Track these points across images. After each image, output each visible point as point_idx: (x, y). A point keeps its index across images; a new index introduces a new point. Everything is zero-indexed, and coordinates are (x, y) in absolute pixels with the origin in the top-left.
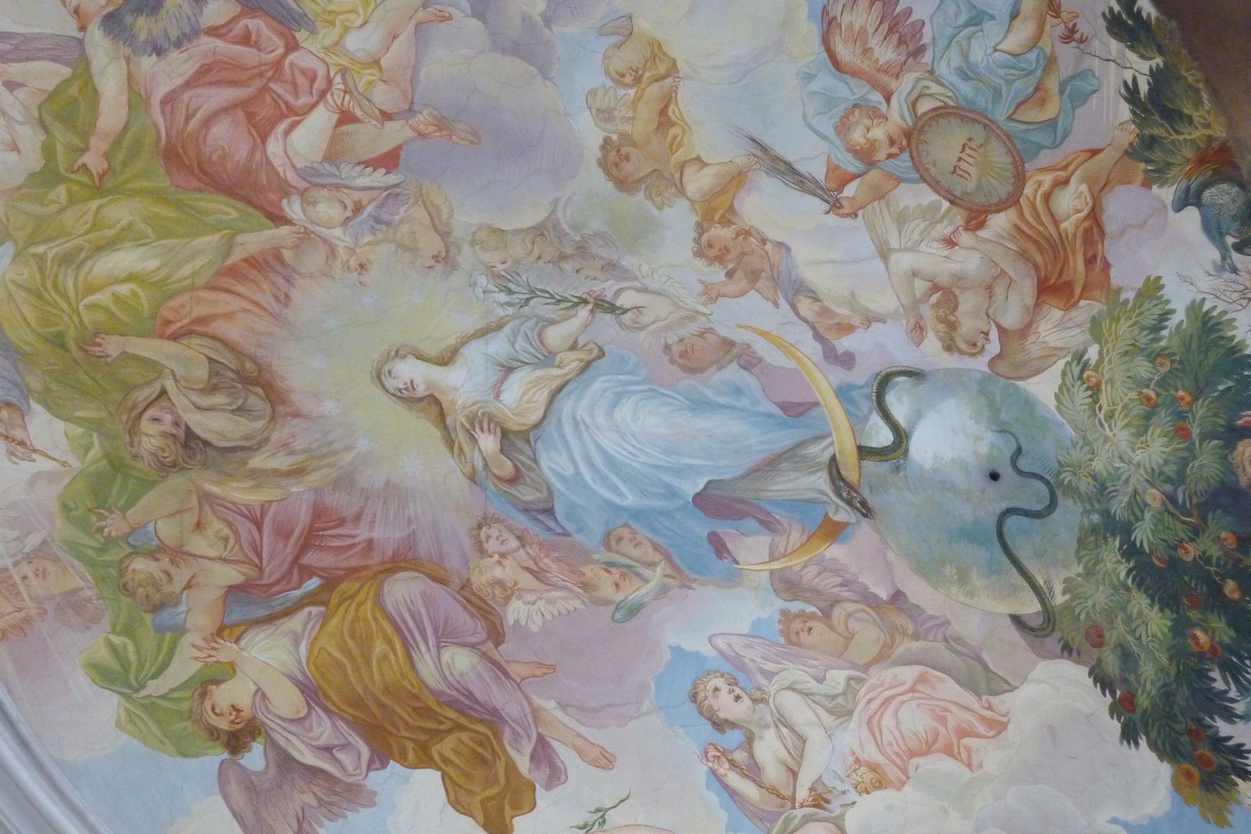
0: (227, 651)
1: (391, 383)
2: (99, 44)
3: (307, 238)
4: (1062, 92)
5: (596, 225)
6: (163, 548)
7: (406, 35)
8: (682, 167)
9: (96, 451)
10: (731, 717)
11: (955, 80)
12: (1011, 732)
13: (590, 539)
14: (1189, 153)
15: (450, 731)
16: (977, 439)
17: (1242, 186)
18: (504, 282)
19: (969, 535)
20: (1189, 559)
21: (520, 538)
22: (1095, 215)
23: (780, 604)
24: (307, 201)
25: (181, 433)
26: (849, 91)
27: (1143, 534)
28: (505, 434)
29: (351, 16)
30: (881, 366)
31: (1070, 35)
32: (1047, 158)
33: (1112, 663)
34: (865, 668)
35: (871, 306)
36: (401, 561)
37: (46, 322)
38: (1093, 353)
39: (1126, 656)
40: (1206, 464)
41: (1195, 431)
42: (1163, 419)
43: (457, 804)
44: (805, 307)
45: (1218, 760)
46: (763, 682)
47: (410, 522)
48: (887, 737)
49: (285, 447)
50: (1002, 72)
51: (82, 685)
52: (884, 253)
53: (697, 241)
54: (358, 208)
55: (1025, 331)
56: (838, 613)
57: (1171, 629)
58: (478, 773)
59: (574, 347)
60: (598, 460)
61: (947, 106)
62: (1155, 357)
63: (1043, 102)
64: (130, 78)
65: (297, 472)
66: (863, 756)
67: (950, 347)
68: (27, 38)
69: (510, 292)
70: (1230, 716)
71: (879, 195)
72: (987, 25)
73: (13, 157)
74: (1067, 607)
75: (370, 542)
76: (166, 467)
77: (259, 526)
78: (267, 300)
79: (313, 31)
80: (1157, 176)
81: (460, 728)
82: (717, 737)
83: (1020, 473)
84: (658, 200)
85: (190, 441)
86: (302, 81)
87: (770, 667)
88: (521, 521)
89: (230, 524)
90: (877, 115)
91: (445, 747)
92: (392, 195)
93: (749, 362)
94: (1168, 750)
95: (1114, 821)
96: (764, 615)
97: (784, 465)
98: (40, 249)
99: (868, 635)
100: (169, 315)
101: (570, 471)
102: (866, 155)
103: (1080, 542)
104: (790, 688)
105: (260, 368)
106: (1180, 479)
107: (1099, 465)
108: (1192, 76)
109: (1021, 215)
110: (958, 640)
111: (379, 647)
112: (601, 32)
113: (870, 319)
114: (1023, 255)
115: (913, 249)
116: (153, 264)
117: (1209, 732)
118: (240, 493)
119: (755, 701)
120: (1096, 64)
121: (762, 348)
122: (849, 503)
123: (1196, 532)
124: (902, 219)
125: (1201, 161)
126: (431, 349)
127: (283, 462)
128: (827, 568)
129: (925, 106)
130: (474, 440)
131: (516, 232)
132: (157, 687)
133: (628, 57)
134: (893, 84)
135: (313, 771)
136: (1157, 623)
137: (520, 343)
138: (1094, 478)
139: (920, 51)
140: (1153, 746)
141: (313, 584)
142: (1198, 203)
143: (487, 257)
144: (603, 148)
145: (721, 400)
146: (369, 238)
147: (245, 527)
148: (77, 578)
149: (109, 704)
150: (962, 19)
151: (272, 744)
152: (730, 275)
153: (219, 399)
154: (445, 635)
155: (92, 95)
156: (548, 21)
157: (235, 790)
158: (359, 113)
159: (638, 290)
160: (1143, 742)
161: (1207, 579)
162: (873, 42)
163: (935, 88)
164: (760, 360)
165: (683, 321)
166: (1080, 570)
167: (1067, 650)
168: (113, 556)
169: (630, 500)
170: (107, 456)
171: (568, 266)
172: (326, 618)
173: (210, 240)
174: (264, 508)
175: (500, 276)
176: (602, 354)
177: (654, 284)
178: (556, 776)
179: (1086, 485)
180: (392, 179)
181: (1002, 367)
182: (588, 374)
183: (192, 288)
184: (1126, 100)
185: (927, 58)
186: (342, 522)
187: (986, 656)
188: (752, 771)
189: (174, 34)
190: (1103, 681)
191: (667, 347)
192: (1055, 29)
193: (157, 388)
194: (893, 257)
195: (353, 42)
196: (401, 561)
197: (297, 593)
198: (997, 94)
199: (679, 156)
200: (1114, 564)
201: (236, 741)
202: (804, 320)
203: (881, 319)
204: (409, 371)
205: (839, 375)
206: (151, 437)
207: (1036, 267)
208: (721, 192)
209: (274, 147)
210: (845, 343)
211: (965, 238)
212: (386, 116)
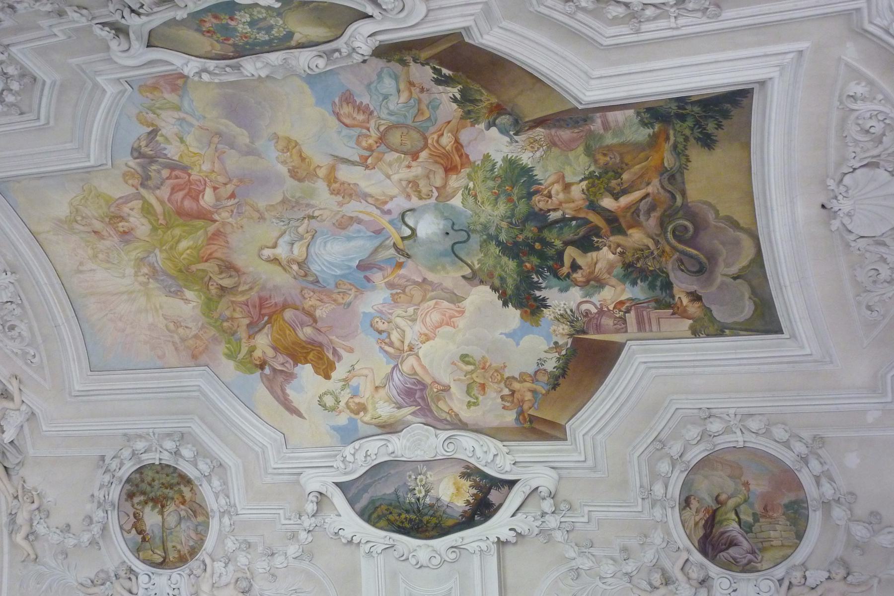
0: (252, 343)
1: (264, 258)
2: (143, 191)
3: (224, 224)
4: (428, 108)
5: (298, 195)
6: (228, 318)
7: (216, 161)
8: (315, 170)
9: (203, 297)
10: (383, 329)
11: (389, 117)
12: (467, 314)
13: (332, 286)
14: (485, 111)
15: (311, 351)
16: (438, 224)
17: (510, 114)
18: (280, 219)
19: (443, 254)
20: (521, 240)
21: (313, 292)
22: (457, 141)
23: (389, 292)
24: (219, 214)
25: (219, 287)
26: (355, 132)
27: (503, 237)
28: (298, 263)
29: (199, 161)
30: (402, 211)
31: (422, 90)
32: (432, 129)
33: (497, 283)
34: (419, 304)
35: (391, 194)
36: (285, 306)
37: (176, 267)
38: (471, 185)
39: (502, 279)
40: (522, 208)
41: (515, 198)
42: (503, 198)
43: (317, 372)
44: (370, 200)
45: (535, 304)
46: (390, 316)
47: (284, 295)
48: (428, 324)
49: (245, 283)
50: (403, 109)
51: (224, 360)
52: (388, 177)
53: (330, 190)
54: (232, 211)
55: (444, 186)
56: (407, 290)
57: (517, 266)
58: (320, 362)
59: (307, 232)
60: (326, 264)
61: (389, 126)
62: (494, 179)
63: (422, 114)
64: (157, 198)
65: (251, 289)
66: (422, 332)
67: (421, 198)
68: (127, 196)
69: (283, 221)
70: (540, 289)
71: (380, 159)
72: (391, 98)
73: (144, 227)
74: (480, 269)
75: (276, 303)
76: (220, 297)
77: (248, 306)
78: (223, 244)
79: (192, 169)
80: (476, 121)
81: (313, 350)
82: (380, 336)
83: (456, 231)
84: (312, 182)
85: (222, 288)
86: (198, 183)
87: (391, 311)
88: (312, 286)
89: (241, 307)
90: (367, 136)
91: (311, 356)
92: (239, 205)
93: (359, 221)
94: (519, 305)
95: (501, 334)
96: (386, 296)
97: (380, 250)
98: (164, 248)
99: (417, 293)
100: (202, 255)
101: (319, 269)
102: (370, 149)
103: (481, 246)
104: (398, 316)
105: (230, 264)
106: (513, 215)
107: (482, 220)
108: (476, 86)
109: (430, 150)
110: (446, 288)
111: (288, 332)
112: (269, 140)
113: (392, 198)
114: (436, 162)
115: (398, 173)
116: (191, 243)
117: (533, 296)
118: (241, 299)
119: (388, 323)
120: (437, 96)
121: (361, 216)
122: (403, 256)
123: (522, 230)
124: (390, 165)
125: (491, 111)
126: (270, 244)
127: (246, 287)
129: (382, 128)
130: (291, 268)
131: (277, 204)
132: (241, 356)
133: (282, 144)
134: (368, 125)
135: (282, 371)
136: (511, 265)
137: (292, 235)
138: (481, 225)
139: (371, 113)
140: (514, 306)
141: (266, 318)
142: (494, 125)
143: (273, 214)
144: (289, 172)
145: (355, 235)
146: (239, 219)
147: (244, 307)
148: (213, 332)
149: (231, 364)
150: (381, 99)
151: (270, 365)
152: (343, 197)
153: (224, 275)
154: (302, 325)
155: (151, 205)
156: (252, 143)
157: (264, 380)
158: (217, 186)
159: (319, 210)
160: (510, 305)
161: (528, 245)
162: (355, 115)
163: (383, 122)
164: (363, 220)
165: (335, 215)
166: (483, 255)
167: (482, 282)
168: (218, 323)
169: (339, 272)
170: (206, 298)
171: (296, 209)
172: (272, 327)
173: (201, 232)
174: (247, 300)
175: (278, 218)
176: (316, 232)
177: (322, 207)
178: (340, 358)
179: (479, 228)
180: (237, 200)
181: (440, 199)
182: (315, 238)
183: (203, 246)
184: (455, 102)
185: (375, 114)
186: (267, 300)
187: (456, 292)
188: (391, 344)
189: (159, 183)
190: (494, 289)
191: (334, 224)
192: (415, 91)
193: (208, 277)
194: (392, 177)
195: (204, 168)
196: (285, 306)
197: (263, 322)
198: (405, 116)
199: (312, 168)
200: (494, 250)
201: (262, 367)
202: (371, 204)
203: (395, 197)
204: (267, 253)
205: (388, 217)
206: (214, 290)
207: (442, 165)
208: (330, 173)
209: (202, 202)
210: (386, 207)
211: (414, 164)
212: (225, 184)
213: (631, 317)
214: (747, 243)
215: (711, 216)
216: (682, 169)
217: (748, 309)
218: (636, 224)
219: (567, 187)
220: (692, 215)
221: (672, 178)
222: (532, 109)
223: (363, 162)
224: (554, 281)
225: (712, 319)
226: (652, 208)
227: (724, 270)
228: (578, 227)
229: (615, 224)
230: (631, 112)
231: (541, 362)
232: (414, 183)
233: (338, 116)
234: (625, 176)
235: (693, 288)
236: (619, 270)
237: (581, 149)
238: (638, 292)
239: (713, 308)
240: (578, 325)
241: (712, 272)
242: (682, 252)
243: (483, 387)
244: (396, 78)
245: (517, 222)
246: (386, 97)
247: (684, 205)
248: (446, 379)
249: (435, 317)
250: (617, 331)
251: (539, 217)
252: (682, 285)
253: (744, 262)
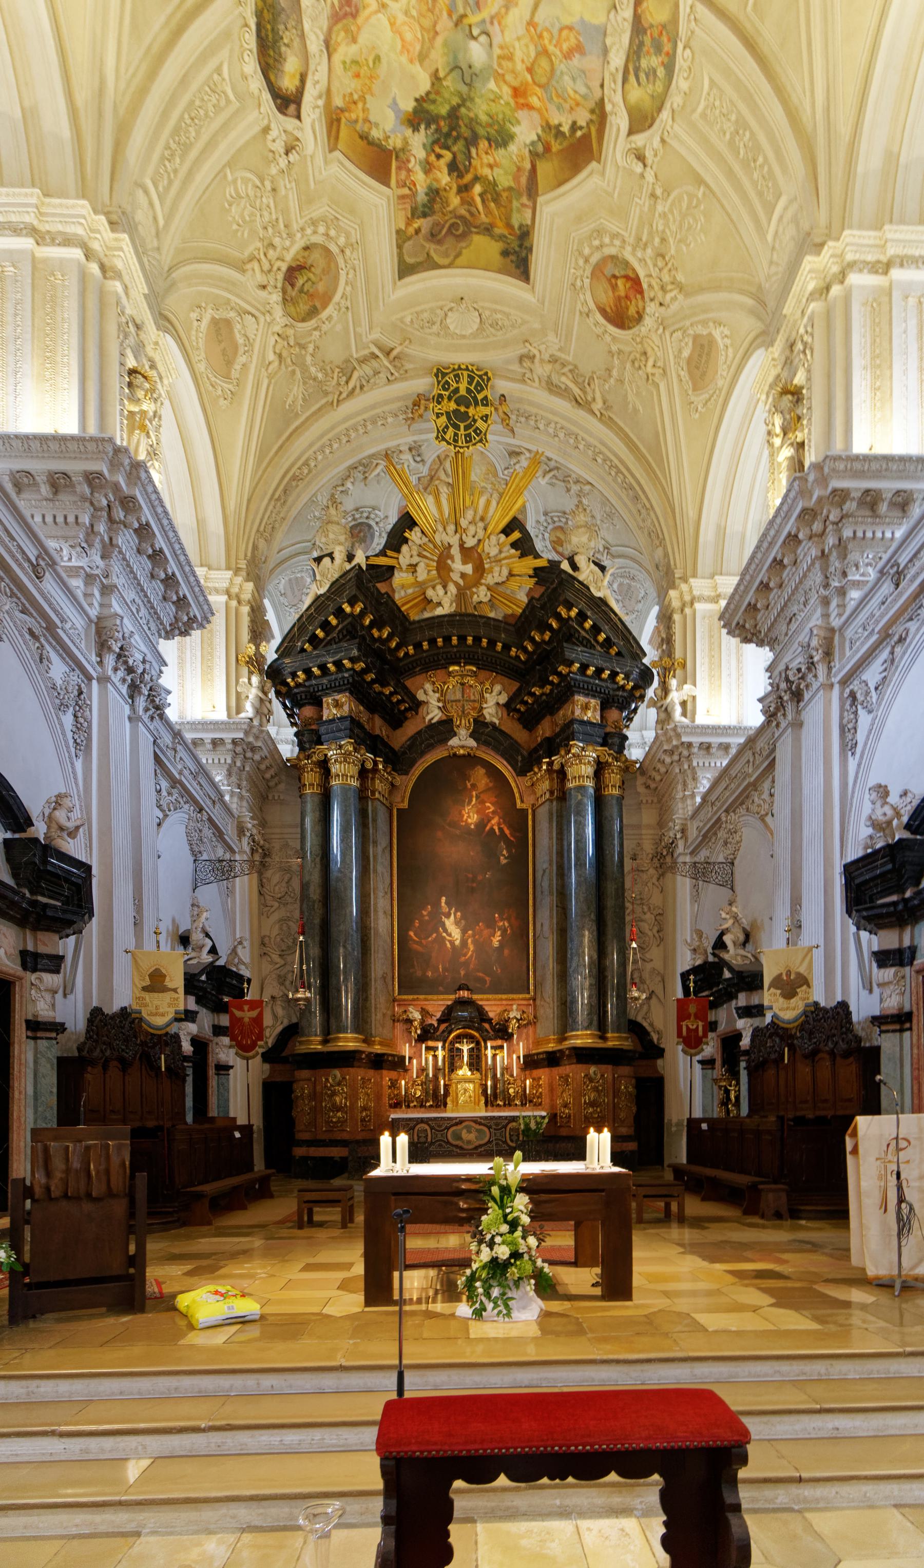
19: (455, 58)
30: (491, 34)
40: (481, 132)
52: (519, 39)
55: (505, 81)
62: (503, 120)
67: (499, 57)
71: (532, 39)
90: (550, 41)
94: (416, 111)
99: (427, 23)
102: (540, 36)
108: (565, 144)
124: (527, 46)
128: (441, 11)
136: (444, 110)
167: (433, 84)
190: (428, 93)
200: (455, 101)
205: (488, 20)
210: (496, 23)
213: (406, 191)
214: (446, 261)
215: (463, 244)
216: (492, 236)
217: (410, 260)
218: (463, 202)
219: (491, 167)
220: (464, 236)
221: (487, 230)
222: (545, 169)
223: (531, 23)
224: (430, 140)
225: (404, 242)
226: (472, 214)
228: (465, 166)
229: (464, 189)
230: (529, 222)
231: (377, 125)
232: (510, 58)
233: (570, 28)
234: (492, 205)
235: (423, 231)
236: (435, 185)
237: (512, 184)
238: (421, 197)
240: (401, 154)
241: (432, 241)
242: (443, 226)
243: (357, 76)
244: (585, 97)
245: (473, 122)
246: (574, 79)
248: (363, 39)
249: (409, 36)
250: (397, 182)
251: (472, 141)
252: (423, 224)
253: (436, 258)
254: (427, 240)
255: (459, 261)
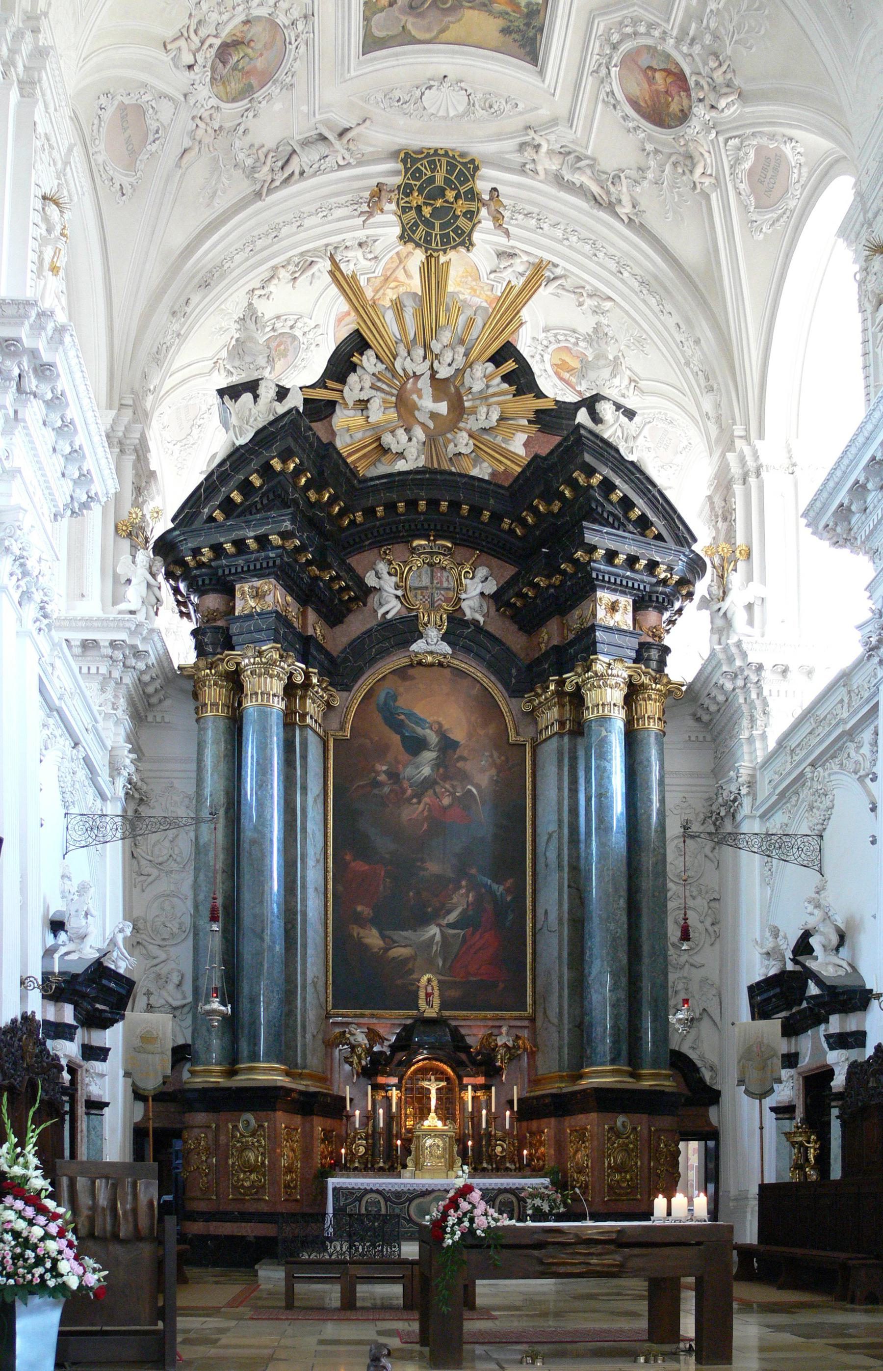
214: (428, 36)
215: (450, 19)
216: (490, 12)
227: (411, 23)
239: (383, 14)
241: (409, 14)
247: (462, 6)
254: (402, 11)
255: (444, 36)
